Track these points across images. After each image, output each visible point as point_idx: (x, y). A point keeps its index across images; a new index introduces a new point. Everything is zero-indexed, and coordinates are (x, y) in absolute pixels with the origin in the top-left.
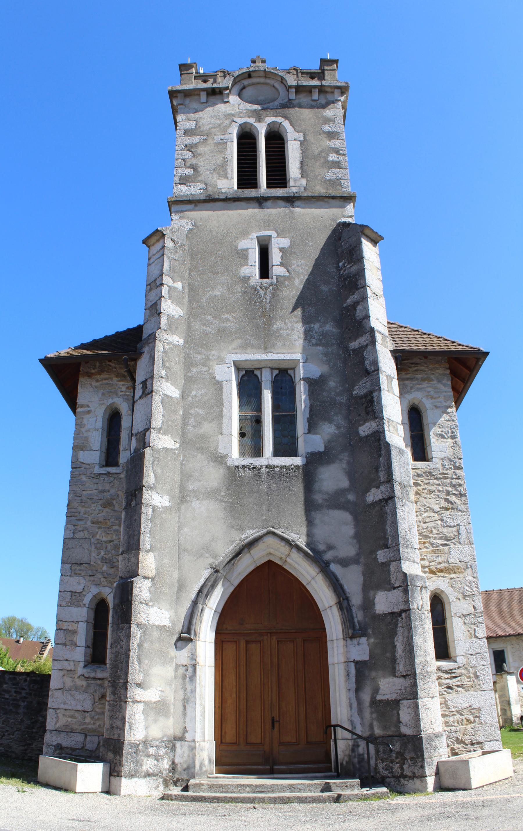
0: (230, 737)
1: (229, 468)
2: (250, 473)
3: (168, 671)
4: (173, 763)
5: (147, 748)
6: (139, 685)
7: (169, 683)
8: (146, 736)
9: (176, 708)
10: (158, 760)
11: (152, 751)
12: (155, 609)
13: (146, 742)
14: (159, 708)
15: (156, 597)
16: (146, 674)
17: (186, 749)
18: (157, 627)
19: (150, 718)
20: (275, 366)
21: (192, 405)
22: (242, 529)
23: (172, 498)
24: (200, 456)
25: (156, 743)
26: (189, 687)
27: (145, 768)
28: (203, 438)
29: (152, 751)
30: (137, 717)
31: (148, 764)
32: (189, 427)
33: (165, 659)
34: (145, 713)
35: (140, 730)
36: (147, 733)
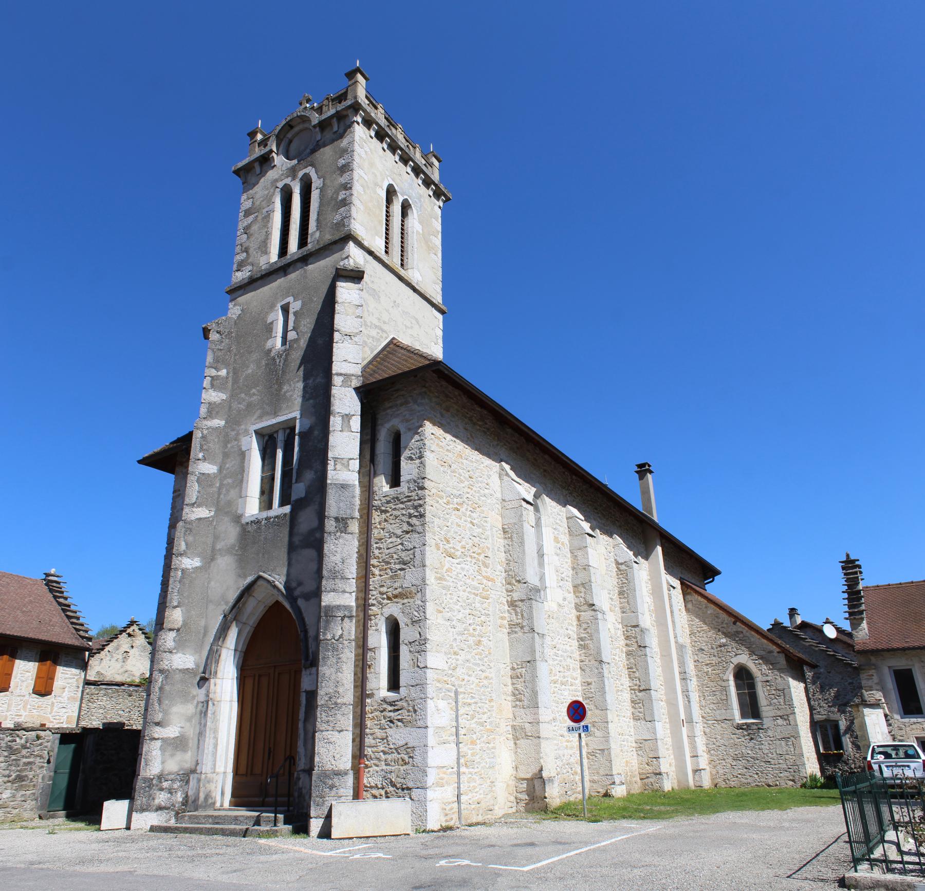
0: (243, 770)
1: (242, 525)
2: (255, 526)
3: (190, 709)
4: (187, 796)
5: (161, 782)
6: (158, 724)
7: (189, 719)
8: (162, 771)
9: (192, 743)
10: (171, 793)
11: (165, 785)
13: (161, 777)
14: (178, 744)
16: (166, 713)
17: (195, 781)
18: (180, 670)
19: (167, 754)
20: (285, 426)
21: (225, 477)
22: (245, 577)
23: (203, 559)
24: (226, 519)
25: (170, 777)
26: (203, 722)
27: (157, 802)
28: (229, 503)
30: (154, 753)
31: (161, 798)
32: (222, 496)
33: (185, 697)
34: (162, 749)
35: (156, 764)
36: (163, 768)
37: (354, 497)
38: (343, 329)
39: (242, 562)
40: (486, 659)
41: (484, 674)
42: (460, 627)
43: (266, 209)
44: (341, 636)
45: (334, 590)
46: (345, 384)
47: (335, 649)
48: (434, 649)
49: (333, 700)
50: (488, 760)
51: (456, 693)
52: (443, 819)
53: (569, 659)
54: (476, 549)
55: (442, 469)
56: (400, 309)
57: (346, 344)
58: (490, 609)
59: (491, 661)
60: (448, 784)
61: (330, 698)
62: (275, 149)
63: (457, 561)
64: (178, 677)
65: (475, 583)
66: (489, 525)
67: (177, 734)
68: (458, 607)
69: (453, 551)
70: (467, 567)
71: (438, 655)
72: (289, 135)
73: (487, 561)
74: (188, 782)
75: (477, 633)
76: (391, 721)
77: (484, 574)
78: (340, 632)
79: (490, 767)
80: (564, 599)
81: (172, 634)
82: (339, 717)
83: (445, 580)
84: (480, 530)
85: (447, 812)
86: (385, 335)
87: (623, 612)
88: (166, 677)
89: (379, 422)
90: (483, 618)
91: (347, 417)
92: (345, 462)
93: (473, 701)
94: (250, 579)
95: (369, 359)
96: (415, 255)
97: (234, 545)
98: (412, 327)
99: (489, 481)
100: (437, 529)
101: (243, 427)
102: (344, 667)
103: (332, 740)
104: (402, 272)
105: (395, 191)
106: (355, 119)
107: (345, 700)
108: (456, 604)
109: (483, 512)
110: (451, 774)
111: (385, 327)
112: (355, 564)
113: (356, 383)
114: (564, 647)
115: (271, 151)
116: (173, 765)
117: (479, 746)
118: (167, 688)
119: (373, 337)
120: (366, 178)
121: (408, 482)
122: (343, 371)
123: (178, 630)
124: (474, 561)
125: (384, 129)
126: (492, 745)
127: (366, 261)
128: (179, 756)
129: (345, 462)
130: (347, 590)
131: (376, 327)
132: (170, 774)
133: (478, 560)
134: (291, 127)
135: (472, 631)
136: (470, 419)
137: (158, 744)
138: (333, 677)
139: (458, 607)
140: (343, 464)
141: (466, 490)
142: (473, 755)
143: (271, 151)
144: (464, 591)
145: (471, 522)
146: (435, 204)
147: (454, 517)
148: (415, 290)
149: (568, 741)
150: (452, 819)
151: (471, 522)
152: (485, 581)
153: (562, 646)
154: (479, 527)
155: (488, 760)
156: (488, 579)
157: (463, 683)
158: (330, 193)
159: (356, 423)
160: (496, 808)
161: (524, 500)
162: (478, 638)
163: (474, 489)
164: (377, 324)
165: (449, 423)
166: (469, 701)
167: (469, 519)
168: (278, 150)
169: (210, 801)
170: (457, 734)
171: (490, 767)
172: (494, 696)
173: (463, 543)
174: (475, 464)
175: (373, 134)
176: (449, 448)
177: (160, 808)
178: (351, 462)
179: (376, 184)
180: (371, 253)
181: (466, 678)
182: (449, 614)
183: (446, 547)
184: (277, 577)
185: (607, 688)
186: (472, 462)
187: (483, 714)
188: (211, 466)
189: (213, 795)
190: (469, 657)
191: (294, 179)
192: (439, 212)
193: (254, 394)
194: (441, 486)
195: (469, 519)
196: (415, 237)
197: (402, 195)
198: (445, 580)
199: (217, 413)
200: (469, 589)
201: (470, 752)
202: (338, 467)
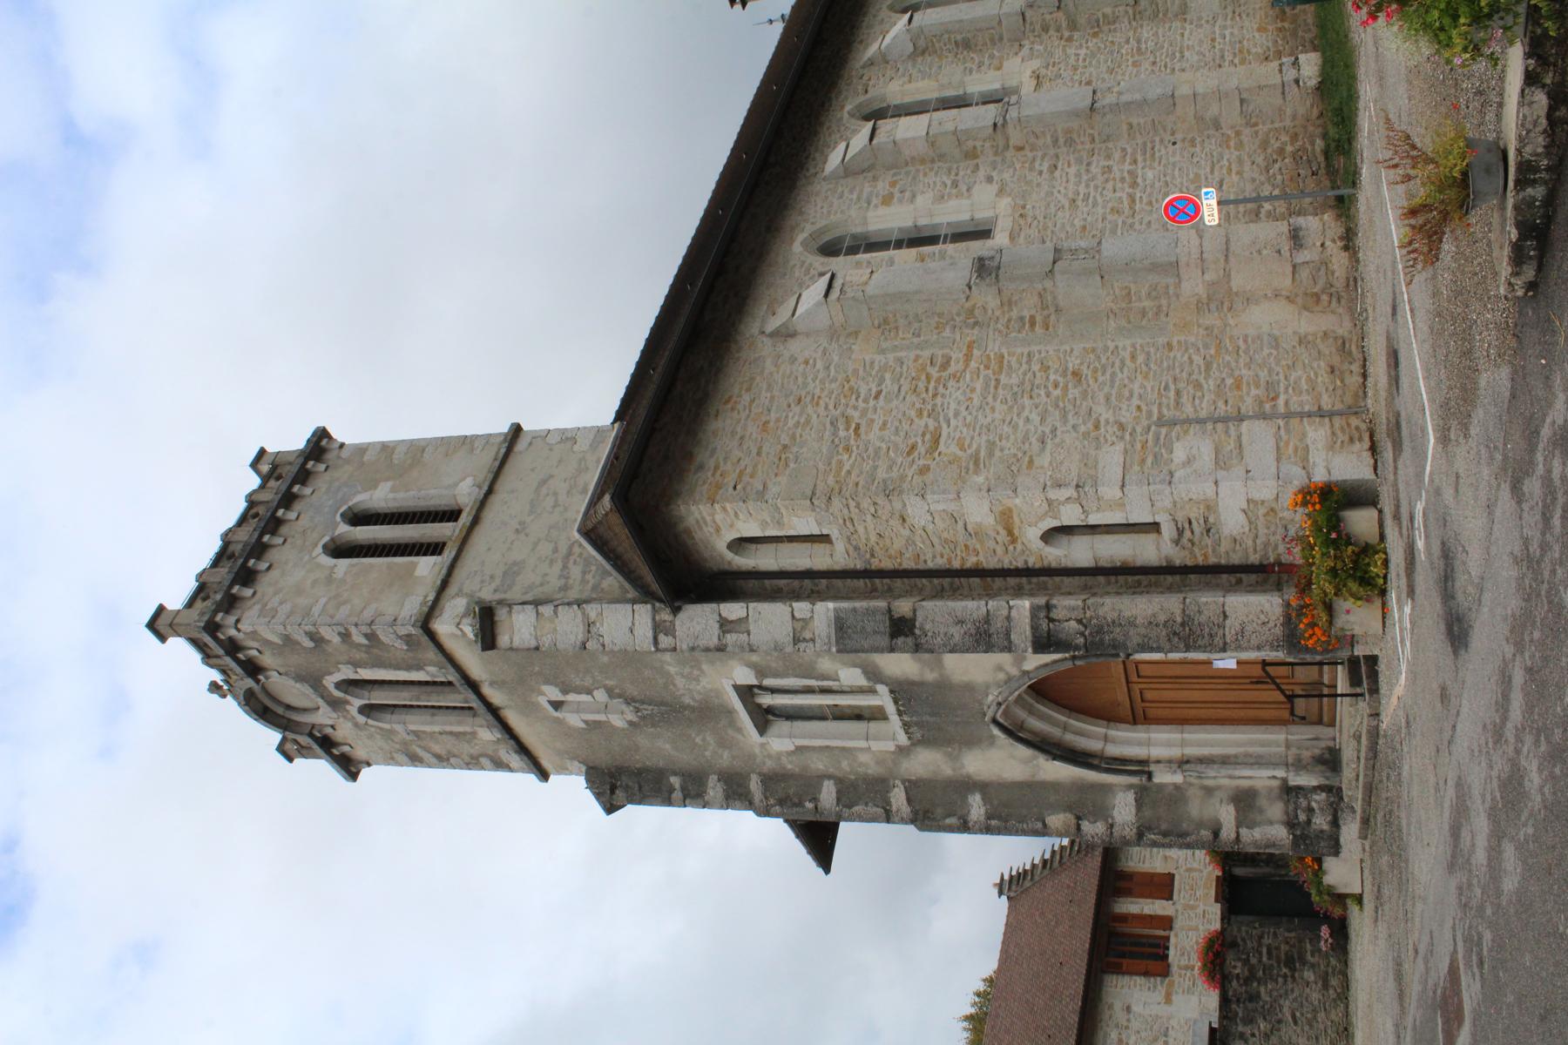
6: (1216, 834)
11: (1302, 817)
12: (1115, 813)
13: (1291, 824)
15: (1101, 812)
16: (1200, 824)
19: (1258, 818)
27: (1326, 827)
29: (1302, 817)
31: (1321, 822)
37: (854, 610)
39: (971, 742)
40: (1104, 361)
41: (1128, 362)
42: (1054, 417)
43: (405, 735)
44: (1080, 621)
45: (1008, 634)
46: (670, 631)
47: (1100, 630)
48: (1092, 472)
49: (1178, 629)
50: (1266, 351)
51: (1161, 422)
52: (1357, 445)
53: (1093, 168)
54: (921, 385)
55: (792, 465)
56: (528, 520)
57: (602, 630)
58: (1019, 350)
59: (1106, 348)
60: (1304, 435)
61: (1175, 633)
63: (944, 426)
64: (1148, 813)
65: (979, 385)
66: (878, 358)
67: (1231, 809)
68: (1021, 423)
69: (928, 437)
70: (953, 406)
71: (1100, 465)
72: (280, 710)
73: (939, 361)
74: (1299, 788)
75: (1061, 379)
76: (1208, 531)
77: (961, 366)
78: (1073, 624)
79: (1277, 347)
80: (990, 179)
81: (1086, 826)
82: (1203, 619)
83: (978, 451)
84: (888, 376)
85: (1346, 438)
86: (576, 550)
87: (1001, 39)
88: (1149, 829)
89: (726, 567)
90: (1036, 367)
91: (725, 625)
92: (799, 625)
93: (1172, 387)
94: (996, 731)
95: (621, 579)
96: (432, 492)
97: (949, 755)
98: (555, 494)
99: (801, 360)
100: (894, 474)
101: (757, 751)
102: (1127, 614)
103: (1238, 628)
104: (465, 519)
107: (1178, 612)
108: (1015, 427)
109: (856, 371)
110: (1288, 431)
111: (563, 549)
112: (964, 603)
114: (1072, 179)
116: (1276, 810)
117: (1244, 372)
118: (1164, 827)
119: (584, 573)
120: (323, 600)
121: (819, 524)
122: (650, 634)
123: (1079, 818)
124: (941, 390)
126: (1241, 343)
127: (459, 594)
128: (1262, 802)
129: (799, 625)
130: (1005, 612)
131: (565, 567)
132: (1287, 813)
133: (938, 380)
135: (1057, 392)
137: (1244, 831)
138: (1143, 631)
139: (1021, 423)
140: (803, 628)
141: (821, 410)
142: (1257, 387)
144: (993, 409)
145: (876, 397)
146: (339, 457)
147: (871, 436)
148: (490, 491)
149: (1230, 170)
150: (1357, 428)
151: (876, 397)
152: (973, 364)
153: (1071, 186)
154: (882, 381)
155: (1266, 351)
156: (968, 357)
157: (1144, 408)
158: (359, 655)
159: (733, 610)
160: (1340, 332)
161: (826, 295)
162: (1070, 377)
163: (817, 392)
164: (559, 564)
166: (1172, 394)
167: (872, 403)
169: (1327, 756)
170: (1225, 420)
171: (1277, 347)
172: (1162, 340)
173: (913, 413)
175: (248, 592)
176: (755, 451)
177: (1335, 823)
178: (797, 615)
179: (330, 580)
180: (445, 584)
181: (1135, 401)
182: (1033, 440)
183: (923, 451)
184: (990, 698)
185: (1138, 96)
186: (773, 398)
187: (1191, 361)
188: (825, 789)
189: (1317, 752)
190: (1101, 397)
191: (347, 702)
193: (704, 740)
194: (821, 466)
195: (872, 403)
196: (401, 495)
197: (336, 526)
198: (978, 451)
199: (740, 785)
200: (990, 399)
201: (1254, 392)
202: (808, 635)
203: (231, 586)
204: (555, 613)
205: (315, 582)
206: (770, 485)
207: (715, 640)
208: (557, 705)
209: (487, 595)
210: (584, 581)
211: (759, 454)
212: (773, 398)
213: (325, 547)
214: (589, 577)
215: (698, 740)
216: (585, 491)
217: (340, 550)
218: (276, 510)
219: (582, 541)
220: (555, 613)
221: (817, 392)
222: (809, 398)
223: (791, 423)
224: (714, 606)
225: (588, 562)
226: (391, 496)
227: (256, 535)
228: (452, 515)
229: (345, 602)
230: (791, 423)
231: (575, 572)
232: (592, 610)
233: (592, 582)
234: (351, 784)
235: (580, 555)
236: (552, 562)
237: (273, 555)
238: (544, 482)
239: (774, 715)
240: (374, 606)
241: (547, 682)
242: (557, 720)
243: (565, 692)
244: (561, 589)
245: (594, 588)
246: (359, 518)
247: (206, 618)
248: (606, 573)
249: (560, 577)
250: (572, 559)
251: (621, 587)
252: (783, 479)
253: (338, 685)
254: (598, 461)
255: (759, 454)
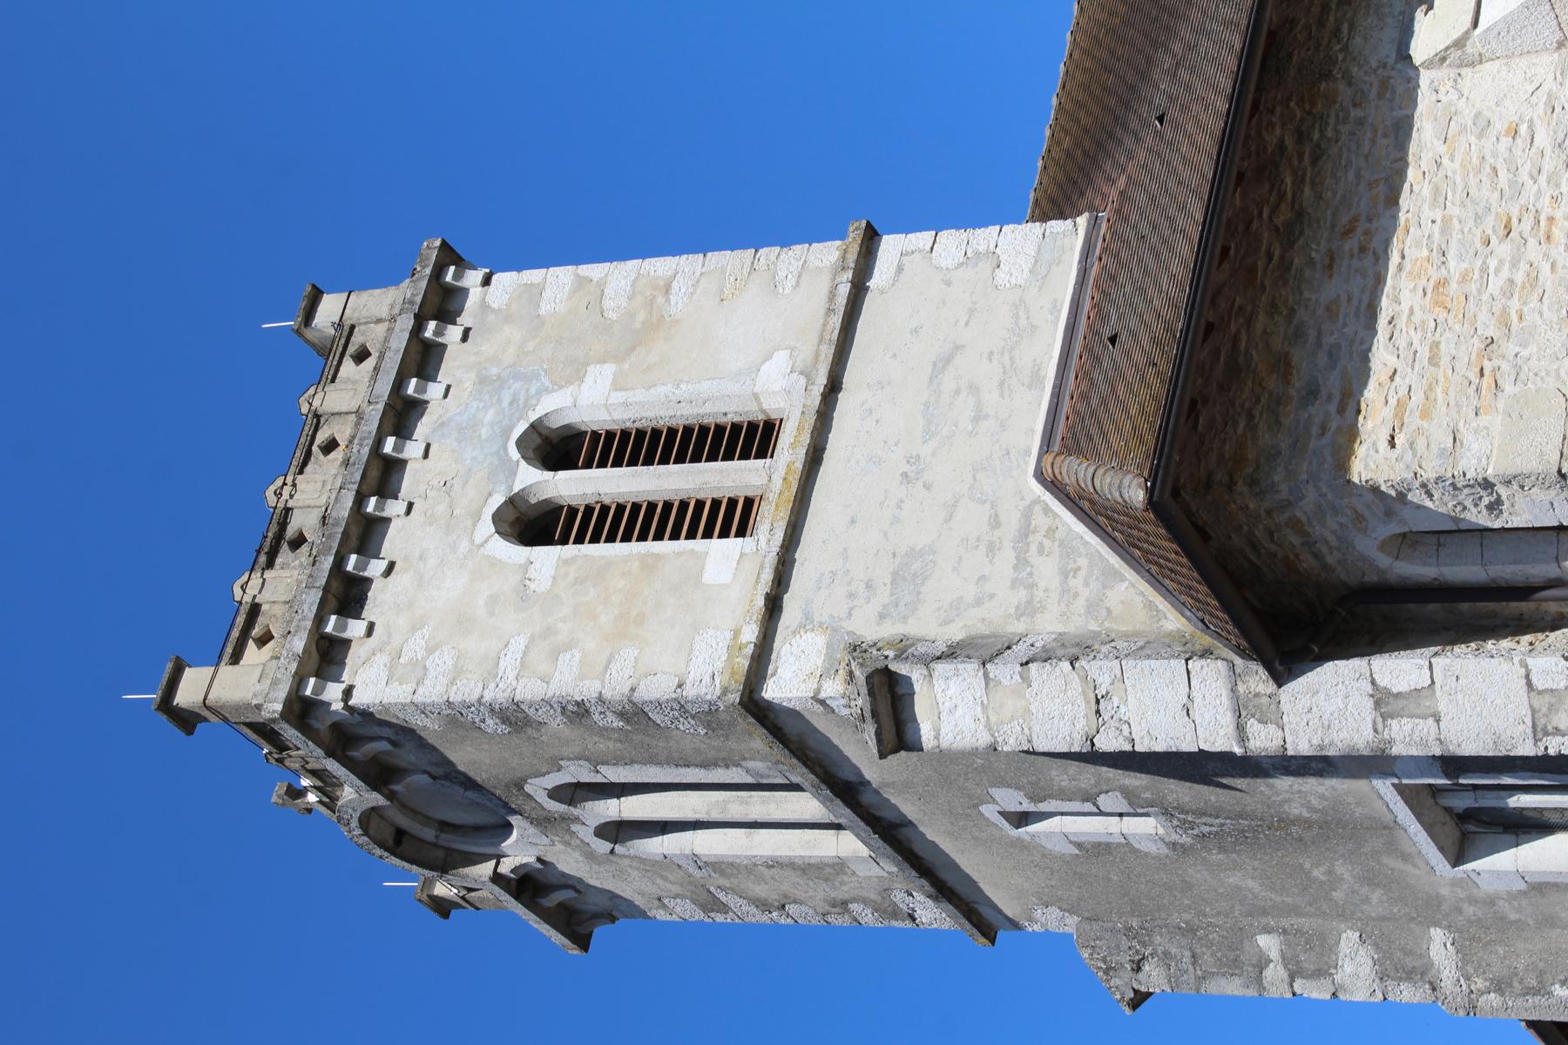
38: (1081, 725)
43: (692, 870)
55: (1508, 387)
57: (1129, 711)
62: (486, 869)
72: (429, 834)
86: (1040, 520)
89: (1372, 578)
91: (1384, 702)
96: (706, 388)
98: (973, 389)
99: (1499, 126)
105: (512, 502)
106: (337, 706)
111: (1012, 521)
113: (1257, 680)
115: (497, 878)
119: (1065, 574)
122: (1227, 720)
125: (326, 589)
127: (807, 623)
131: (1021, 561)
134: (400, 834)
136: (1289, 235)
143: (497, 878)
146: (484, 306)
158: (603, 746)
159: (1400, 669)
164: (1007, 556)
165: (1333, 356)
168: (484, 858)
174: (1453, 210)
175: (355, 628)
180: (773, 606)
186: (1446, 220)
191: (577, 820)
192: (502, 279)
193: (1330, 872)
196: (639, 395)
197: (513, 473)
203: (320, 620)
204: (1025, 679)
205: (493, 600)
206: (1466, 436)
207: (1368, 733)
208: (1021, 819)
209: (870, 630)
210: (1067, 594)
211: (1433, 360)
212: (1446, 220)
213: (497, 518)
214: (1076, 583)
215: (1316, 873)
216: (1036, 380)
217: (534, 525)
218: (379, 442)
219: (1048, 497)
220: (1025, 679)
221: (1546, 200)
222: (1528, 223)
223: (1495, 285)
224: (1357, 664)
225: (1067, 550)
226: (618, 397)
227: (348, 500)
228: (754, 438)
229: (568, 646)
230: (1495, 285)
231: (1046, 570)
232: (1101, 671)
233: (1085, 593)
234: (575, 951)
235: (1050, 532)
236: (992, 549)
237: (393, 543)
238: (944, 362)
239: (1482, 823)
240: (629, 654)
241: (1002, 783)
242: (1019, 844)
243: (1034, 798)
244: (1020, 613)
245: (1092, 607)
246: (558, 448)
247: (282, 692)
248: (1111, 575)
249: (1014, 583)
250: (1035, 539)
251: (1150, 605)
252: (1494, 421)
253: (556, 793)
254: (1055, 309)
255: (1433, 360)
